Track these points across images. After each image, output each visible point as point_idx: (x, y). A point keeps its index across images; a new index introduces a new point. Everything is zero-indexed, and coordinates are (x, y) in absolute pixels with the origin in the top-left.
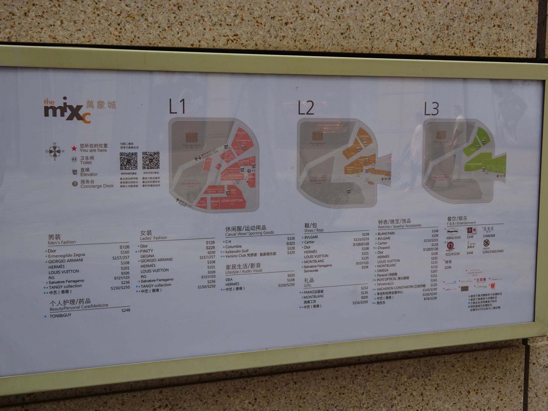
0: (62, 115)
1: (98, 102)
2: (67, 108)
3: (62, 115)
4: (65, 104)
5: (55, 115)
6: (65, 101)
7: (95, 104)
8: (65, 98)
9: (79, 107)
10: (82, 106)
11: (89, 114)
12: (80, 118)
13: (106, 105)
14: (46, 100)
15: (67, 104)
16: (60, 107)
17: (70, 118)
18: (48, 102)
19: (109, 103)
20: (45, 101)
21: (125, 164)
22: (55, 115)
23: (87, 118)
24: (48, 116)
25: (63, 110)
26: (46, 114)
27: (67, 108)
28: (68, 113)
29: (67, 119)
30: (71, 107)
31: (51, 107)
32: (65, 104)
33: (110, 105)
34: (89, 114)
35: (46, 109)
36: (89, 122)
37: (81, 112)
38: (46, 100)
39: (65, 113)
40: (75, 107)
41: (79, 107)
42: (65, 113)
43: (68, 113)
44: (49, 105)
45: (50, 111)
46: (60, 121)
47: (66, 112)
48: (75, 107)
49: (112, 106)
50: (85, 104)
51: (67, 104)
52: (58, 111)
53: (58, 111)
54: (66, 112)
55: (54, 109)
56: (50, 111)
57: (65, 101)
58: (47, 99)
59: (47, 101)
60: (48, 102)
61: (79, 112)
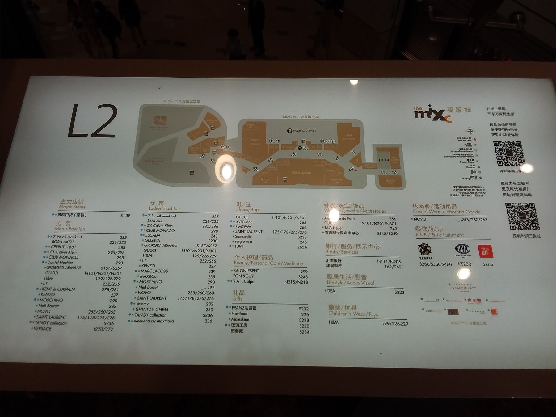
0: (429, 117)
2: (432, 112)
3: (429, 117)
4: (430, 109)
6: (430, 108)
16: (426, 112)
17: (435, 119)
18: (417, 109)
20: (415, 108)
21: (504, 157)
25: (429, 113)
27: (432, 112)
28: (433, 115)
30: (435, 112)
31: (420, 112)
32: (430, 109)
33: (466, 110)
35: (416, 114)
39: (431, 116)
42: (431, 116)
43: (433, 115)
45: (419, 115)
46: (427, 122)
47: (432, 115)
49: (468, 110)
50: (445, 109)
52: (426, 115)
53: (426, 115)
54: (432, 115)
56: (419, 115)
59: (416, 108)
60: (417, 109)
61: (442, 115)
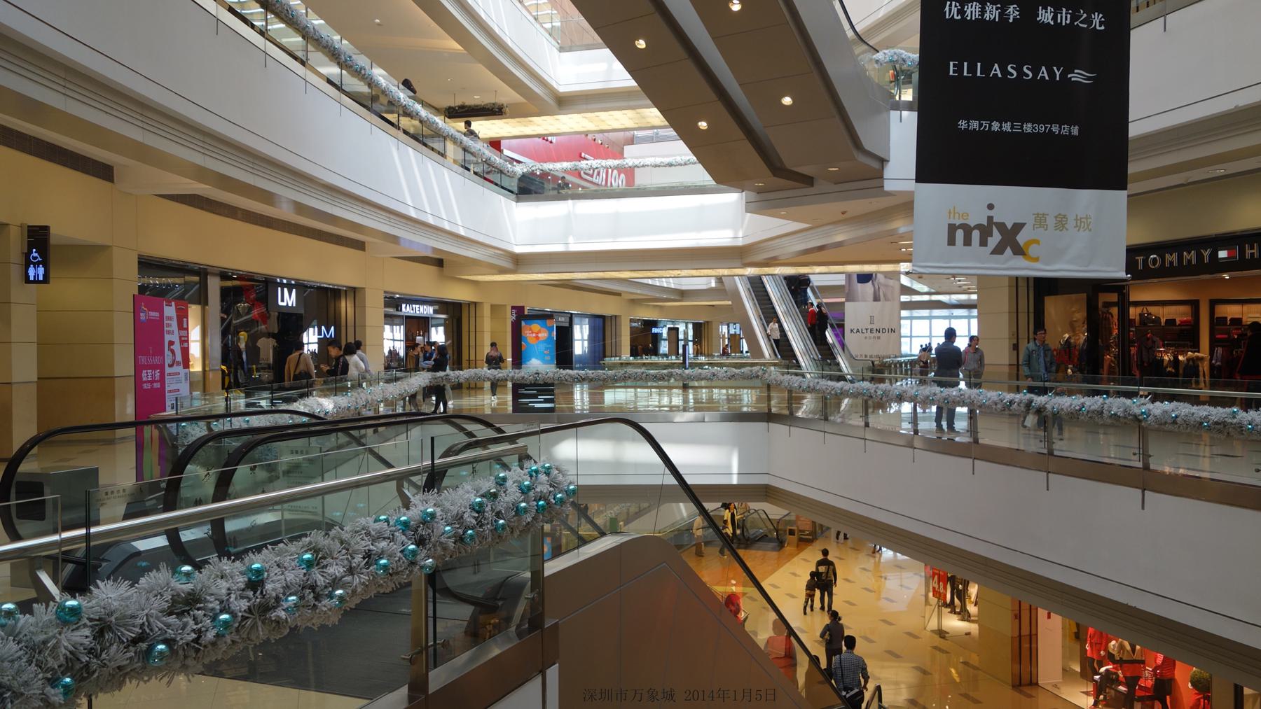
0: (983, 243)
1: (1056, 217)
3: (983, 243)
4: (990, 219)
5: (967, 242)
6: (990, 213)
7: (1051, 221)
8: (991, 207)
9: (1018, 227)
10: (1024, 225)
11: (1037, 242)
12: (1019, 251)
13: (1071, 223)
14: (952, 211)
15: (995, 221)
16: (978, 227)
17: (998, 250)
18: (957, 215)
19: (1076, 220)
20: (950, 213)
22: (967, 242)
23: (1032, 250)
24: (954, 244)
25: (985, 232)
26: (952, 242)
27: (994, 228)
28: (996, 238)
29: (993, 253)
30: (1001, 226)
32: (990, 219)
33: (1079, 224)
34: (1037, 242)
35: (952, 229)
36: (1036, 260)
37: (1021, 238)
38: (952, 211)
39: (989, 238)
40: (1009, 226)
41: (1018, 227)
42: (989, 238)
43: (996, 238)
44: (958, 222)
45: (960, 234)
47: (992, 236)
48: (1009, 226)
51: (995, 221)
52: (976, 235)
53: (976, 235)
54: (992, 236)
55: (968, 230)
56: (960, 234)
57: (990, 213)
58: (954, 208)
59: (954, 213)
60: (957, 215)
